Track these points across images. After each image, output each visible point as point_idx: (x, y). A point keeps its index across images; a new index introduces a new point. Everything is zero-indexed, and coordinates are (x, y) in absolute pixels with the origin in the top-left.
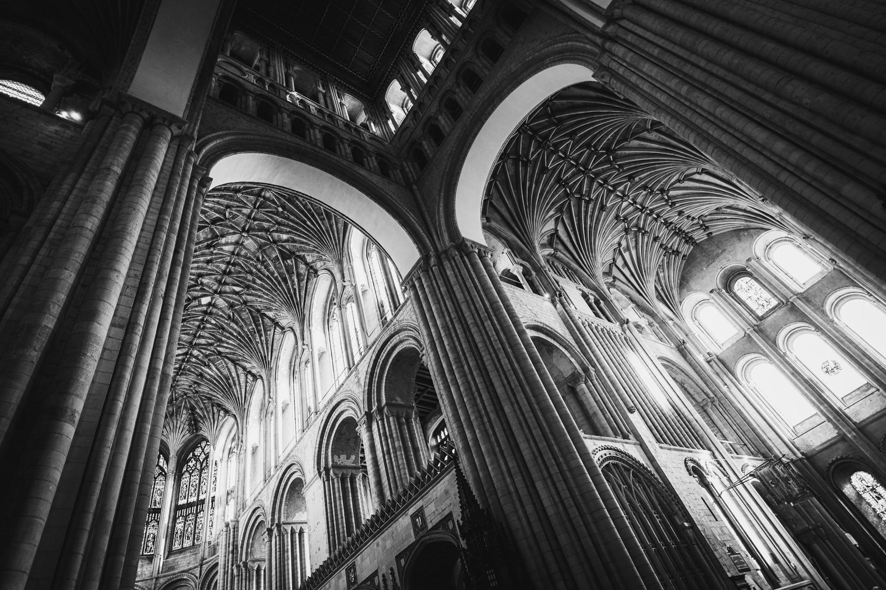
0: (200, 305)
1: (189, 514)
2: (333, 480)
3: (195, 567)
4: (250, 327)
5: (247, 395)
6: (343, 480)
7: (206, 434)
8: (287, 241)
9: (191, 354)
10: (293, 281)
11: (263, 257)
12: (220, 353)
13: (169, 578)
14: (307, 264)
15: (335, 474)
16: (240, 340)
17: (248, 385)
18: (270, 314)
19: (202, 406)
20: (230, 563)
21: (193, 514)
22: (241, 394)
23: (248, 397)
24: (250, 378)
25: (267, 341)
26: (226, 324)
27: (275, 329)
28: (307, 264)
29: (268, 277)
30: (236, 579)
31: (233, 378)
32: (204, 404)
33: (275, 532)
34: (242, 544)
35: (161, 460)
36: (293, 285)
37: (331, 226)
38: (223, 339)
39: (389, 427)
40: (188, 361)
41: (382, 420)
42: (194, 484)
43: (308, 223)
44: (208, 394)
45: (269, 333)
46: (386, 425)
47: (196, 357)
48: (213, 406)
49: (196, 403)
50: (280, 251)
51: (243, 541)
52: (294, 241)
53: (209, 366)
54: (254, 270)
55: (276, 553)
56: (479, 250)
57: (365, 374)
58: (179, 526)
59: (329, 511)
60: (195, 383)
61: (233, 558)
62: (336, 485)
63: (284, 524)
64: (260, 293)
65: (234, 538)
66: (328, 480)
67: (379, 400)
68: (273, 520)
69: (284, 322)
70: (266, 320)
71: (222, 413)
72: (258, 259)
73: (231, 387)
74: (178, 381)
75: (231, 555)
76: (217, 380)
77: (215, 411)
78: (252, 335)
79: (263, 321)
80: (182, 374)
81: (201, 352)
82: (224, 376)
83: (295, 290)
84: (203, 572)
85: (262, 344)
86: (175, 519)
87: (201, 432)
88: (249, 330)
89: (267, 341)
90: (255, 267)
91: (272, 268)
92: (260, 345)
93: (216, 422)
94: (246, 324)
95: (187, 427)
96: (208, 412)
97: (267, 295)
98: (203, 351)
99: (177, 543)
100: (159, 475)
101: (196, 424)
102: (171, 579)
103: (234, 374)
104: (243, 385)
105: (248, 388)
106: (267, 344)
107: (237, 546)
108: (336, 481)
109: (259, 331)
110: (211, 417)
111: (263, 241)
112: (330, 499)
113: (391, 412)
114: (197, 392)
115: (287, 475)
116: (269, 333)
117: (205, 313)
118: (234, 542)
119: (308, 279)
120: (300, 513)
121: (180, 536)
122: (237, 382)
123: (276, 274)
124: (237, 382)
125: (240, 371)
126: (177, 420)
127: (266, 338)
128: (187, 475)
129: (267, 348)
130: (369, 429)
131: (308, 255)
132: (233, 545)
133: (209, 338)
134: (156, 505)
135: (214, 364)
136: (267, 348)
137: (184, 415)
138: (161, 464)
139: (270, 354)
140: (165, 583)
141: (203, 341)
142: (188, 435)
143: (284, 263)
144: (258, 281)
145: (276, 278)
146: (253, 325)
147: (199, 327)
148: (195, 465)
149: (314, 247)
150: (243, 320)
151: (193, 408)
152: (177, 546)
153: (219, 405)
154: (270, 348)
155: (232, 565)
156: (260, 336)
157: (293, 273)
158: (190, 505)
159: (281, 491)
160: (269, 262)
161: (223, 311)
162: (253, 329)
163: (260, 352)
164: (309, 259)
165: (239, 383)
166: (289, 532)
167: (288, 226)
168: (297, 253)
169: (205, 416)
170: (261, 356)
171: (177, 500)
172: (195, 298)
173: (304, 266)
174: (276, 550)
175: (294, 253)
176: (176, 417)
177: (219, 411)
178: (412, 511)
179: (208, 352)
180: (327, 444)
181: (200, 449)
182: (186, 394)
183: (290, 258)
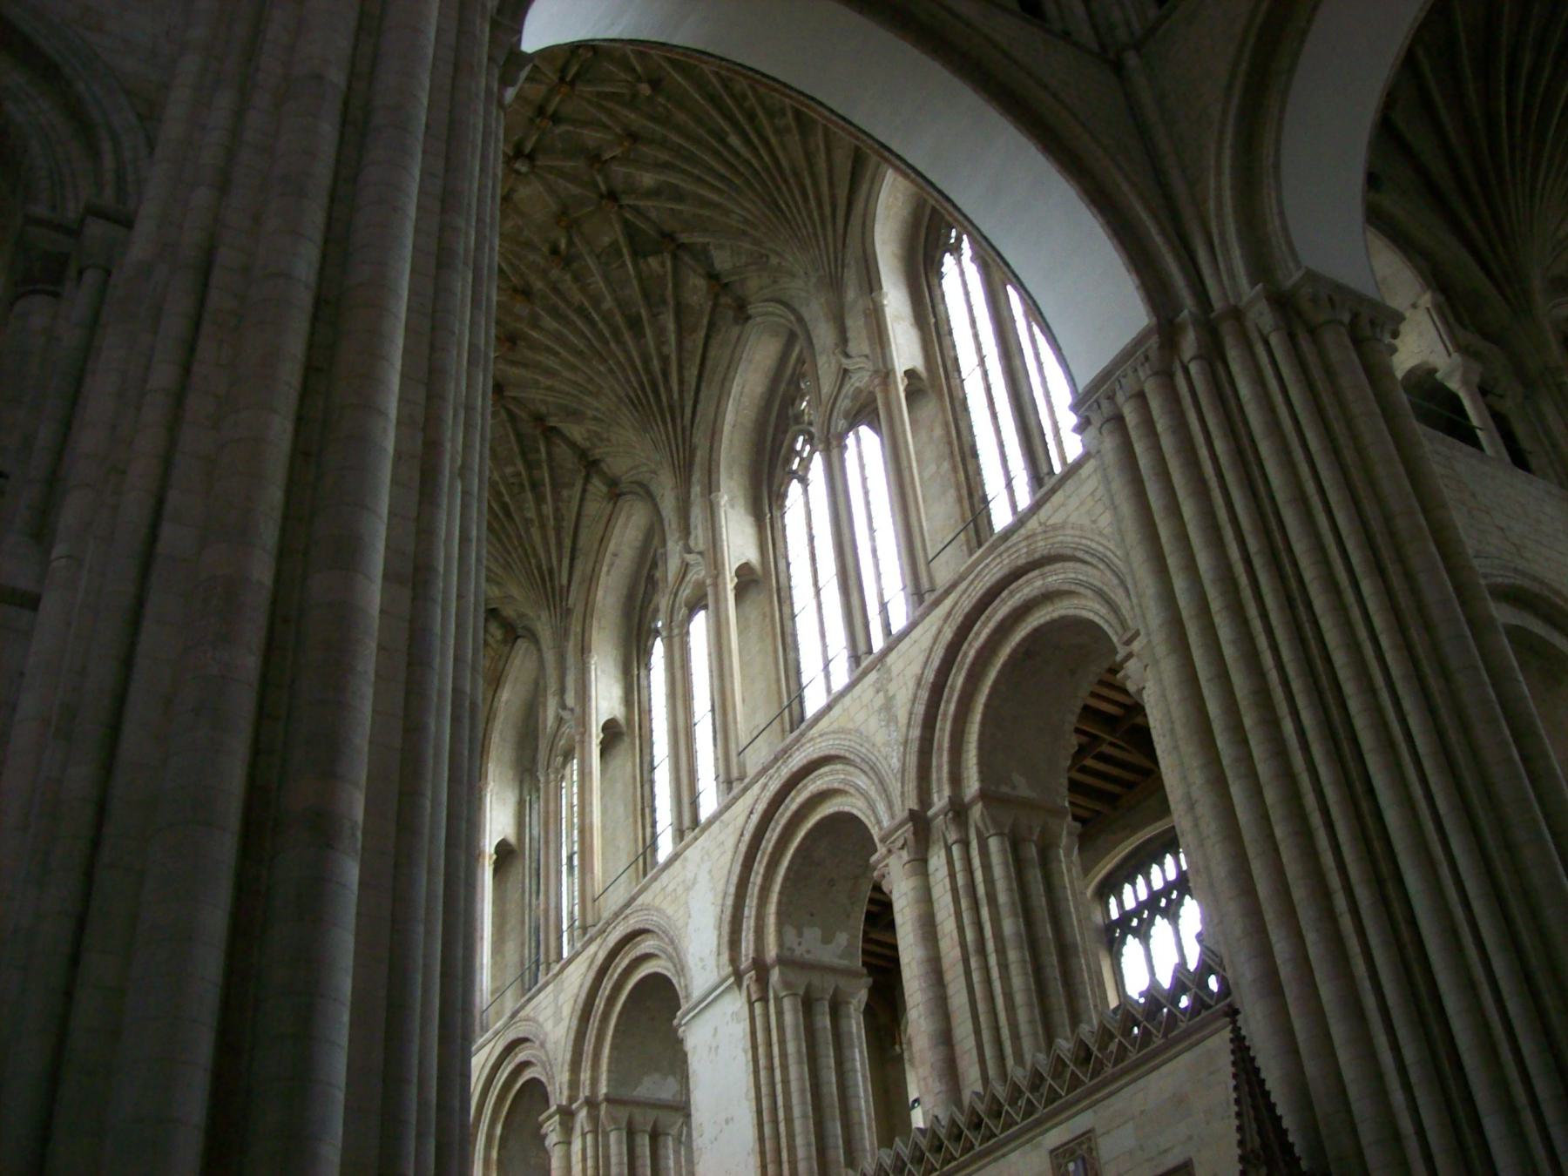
2: (778, 1000)
4: (509, 470)
6: (808, 1005)
8: (656, 193)
10: (661, 332)
11: (570, 243)
14: (713, 276)
15: (787, 984)
18: (577, 433)
24: (497, 632)
25: (559, 518)
27: (587, 480)
28: (713, 276)
29: (581, 311)
36: (661, 342)
37: (809, 156)
39: (987, 867)
41: (965, 844)
43: (734, 140)
45: (565, 493)
46: (976, 862)
50: (627, 224)
52: (678, 195)
54: (538, 285)
56: (1355, 316)
57: (911, 684)
59: (764, 1090)
62: (789, 1018)
64: (551, 362)
66: (764, 999)
67: (956, 779)
68: (574, 1084)
69: (618, 465)
70: (562, 450)
72: (555, 251)
79: (549, 454)
83: (665, 360)
85: (543, 527)
89: (559, 518)
90: (544, 273)
91: (598, 282)
92: (535, 532)
97: (573, 368)
106: (558, 531)
108: (787, 1004)
109: (535, 486)
111: (575, 190)
112: (770, 1057)
113: (997, 823)
115: (623, 962)
116: (565, 493)
119: (712, 326)
120: (657, 1076)
123: (608, 303)
130: (920, 863)
131: (720, 247)
139: (566, 562)
143: (635, 265)
144: (549, 323)
145: (607, 317)
146: (521, 467)
149: (746, 221)
154: (567, 543)
156: (539, 499)
157: (664, 302)
159: (600, 1003)
160: (591, 262)
163: (536, 555)
164: (722, 261)
166: (624, 1124)
167: (663, 143)
168: (684, 238)
170: (539, 568)
173: (701, 283)
175: (669, 237)
178: (1056, 1136)
183: (657, 252)
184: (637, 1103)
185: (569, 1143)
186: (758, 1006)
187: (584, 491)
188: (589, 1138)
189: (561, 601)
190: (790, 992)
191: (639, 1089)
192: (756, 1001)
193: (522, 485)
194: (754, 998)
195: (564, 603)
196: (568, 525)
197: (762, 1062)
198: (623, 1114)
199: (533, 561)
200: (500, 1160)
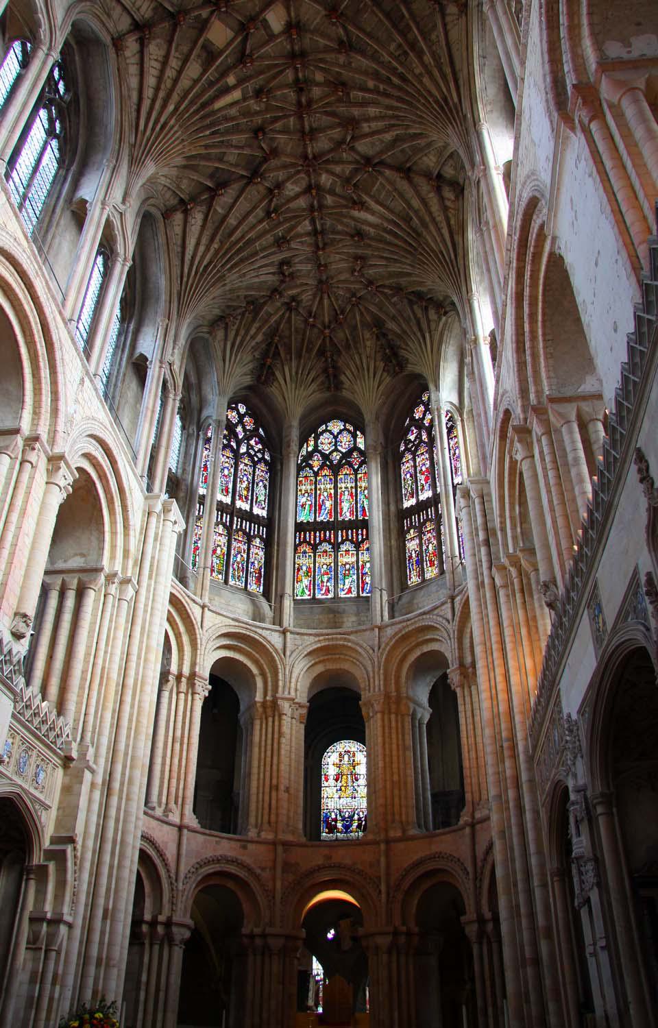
0: (272, 37)
1: (425, 521)
3: (443, 604)
5: (456, 237)
7: (418, 370)
9: (318, 187)
12: (368, 160)
13: (400, 626)
16: (386, 95)
17: (451, 213)
19: (393, 311)
20: (485, 565)
21: (431, 520)
22: (444, 240)
23: (458, 239)
24: (448, 194)
26: (347, 66)
30: (502, 593)
31: (416, 212)
32: (394, 305)
33: (537, 429)
34: (503, 523)
35: (358, 440)
38: (356, 112)
40: (321, 207)
42: (424, 469)
44: (391, 275)
45: (433, 37)
47: (332, 192)
48: (411, 303)
49: (381, 309)
51: (502, 515)
53: (362, 205)
55: (546, 476)
58: (412, 545)
60: (357, 258)
61: (489, 554)
63: (552, 400)
65: (485, 516)
66: (597, 114)
71: (432, 314)
73: (419, 235)
74: (326, 266)
75: (483, 550)
76: (390, 232)
77: (419, 313)
78: (401, 64)
80: (325, 244)
81: (333, 174)
82: (398, 216)
84: (456, 610)
85: (430, 74)
86: (402, 534)
87: (410, 368)
88: (391, 54)
92: (426, 80)
93: (427, 335)
94: (377, 41)
95: (382, 365)
96: (407, 321)
98: (338, 169)
99: (414, 573)
100: (360, 466)
101: (395, 354)
102: (404, 627)
103: (416, 203)
104: (440, 218)
105: (452, 222)
107: (494, 530)
108: (629, 111)
109: (413, 46)
110: (415, 329)
114: (370, 283)
117: (293, 56)
118: (486, 523)
121: (417, 562)
122: (427, 219)
124: (427, 219)
125: (425, 187)
126: (360, 355)
127: (433, 54)
128: (409, 456)
129: (444, 76)
132: (486, 529)
133: (331, 127)
134: (364, 514)
135: (368, 194)
136: (444, 76)
137: (369, 343)
138: (362, 447)
139: (452, 85)
140: (396, 634)
141: (322, 144)
142: (388, 380)
146: (400, 39)
147: (299, 103)
148: (419, 436)
150: (369, 35)
151: (378, 324)
152: (414, 579)
153: (420, 296)
154: (448, 70)
155: (490, 568)
156: (420, 54)
158: (421, 506)
159: (527, 327)
161: (323, 35)
162: (400, 46)
165: (433, 219)
166: (573, 417)
169: (405, 332)
170: (437, 102)
171: (399, 500)
172: (252, 19)
174: (544, 469)
176: (356, 348)
177: (426, 308)
179: (348, 169)
180: (574, 28)
181: (422, 408)
182: (354, 295)
184: (584, 398)
185: (533, 456)
186: (594, 127)
187: (445, 25)
188: (544, 440)
189: (457, 113)
190: (624, 90)
191: (582, 387)
192: (590, 122)
193: (405, 53)
194: (586, 121)
195: (460, 114)
196: (445, 59)
197: (608, 164)
198: (571, 411)
199: (431, 100)
200: (522, 533)
